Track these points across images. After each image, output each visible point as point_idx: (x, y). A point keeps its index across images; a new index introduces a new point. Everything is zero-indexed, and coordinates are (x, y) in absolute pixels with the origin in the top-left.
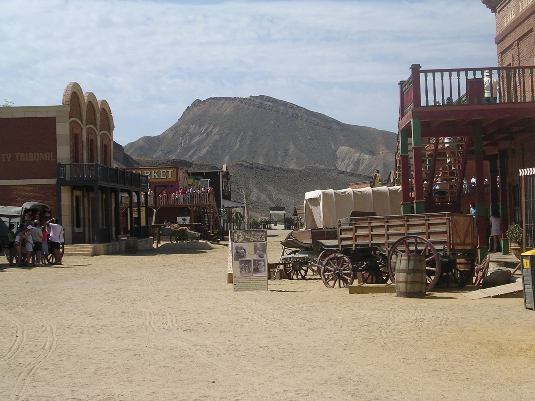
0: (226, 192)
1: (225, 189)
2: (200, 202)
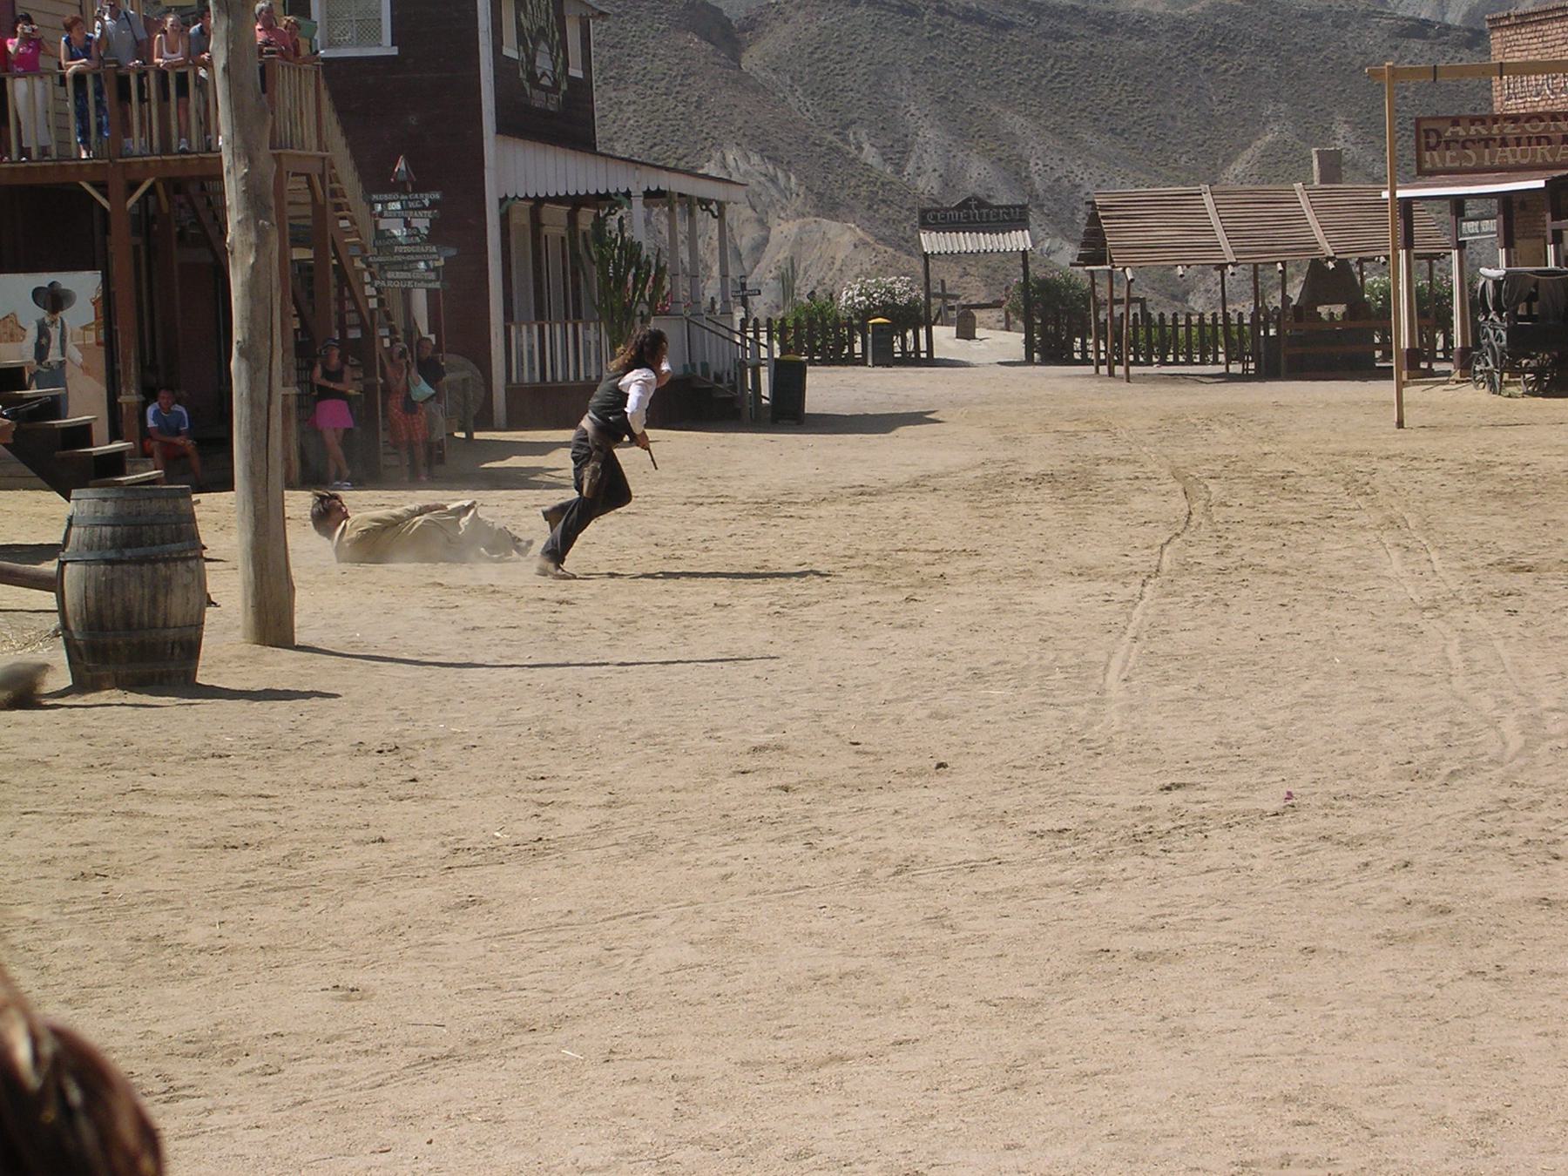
0: (533, 78)
1: (531, 61)
2: (184, 133)
